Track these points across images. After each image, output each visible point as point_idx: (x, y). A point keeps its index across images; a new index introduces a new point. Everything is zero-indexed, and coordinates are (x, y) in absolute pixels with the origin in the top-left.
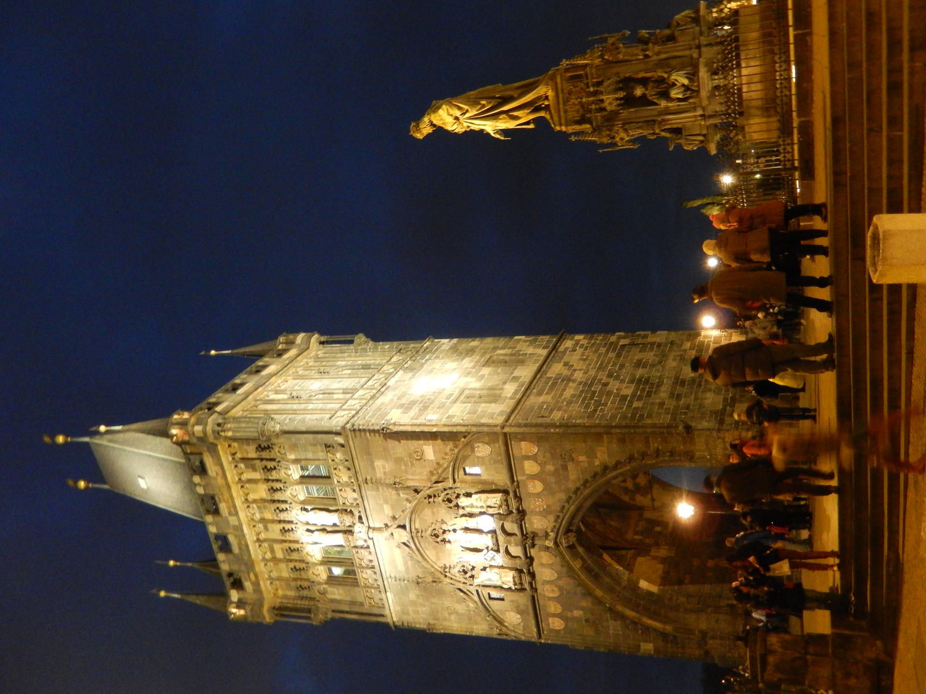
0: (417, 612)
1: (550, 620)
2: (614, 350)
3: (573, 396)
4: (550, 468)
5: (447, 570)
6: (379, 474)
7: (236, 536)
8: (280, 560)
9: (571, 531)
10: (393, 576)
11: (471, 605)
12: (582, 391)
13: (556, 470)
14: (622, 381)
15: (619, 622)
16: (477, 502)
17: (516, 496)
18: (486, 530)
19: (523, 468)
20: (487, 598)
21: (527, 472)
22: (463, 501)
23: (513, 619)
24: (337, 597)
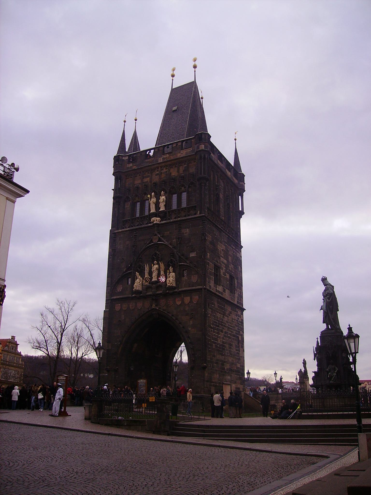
2: (236, 333)
3: (217, 317)
4: (187, 309)
6: (183, 231)
12: (219, 321)
14: (223, 338)
22: (171, 269)
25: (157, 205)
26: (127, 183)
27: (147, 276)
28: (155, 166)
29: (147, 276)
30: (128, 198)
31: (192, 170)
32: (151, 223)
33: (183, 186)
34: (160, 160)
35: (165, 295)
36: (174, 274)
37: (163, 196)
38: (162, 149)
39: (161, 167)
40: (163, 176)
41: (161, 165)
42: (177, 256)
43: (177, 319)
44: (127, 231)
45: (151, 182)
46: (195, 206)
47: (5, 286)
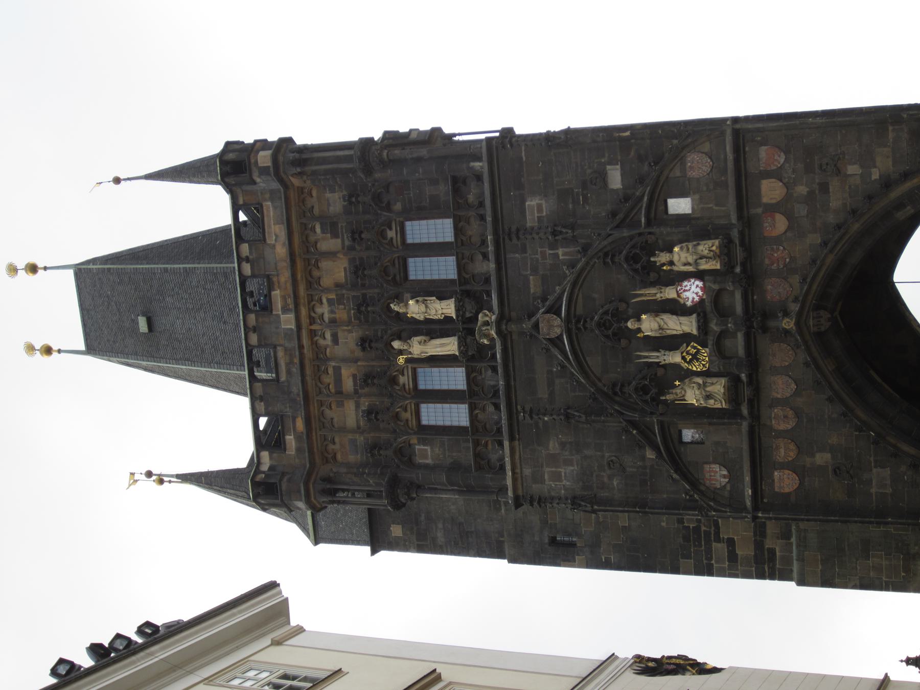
0: (557, 477)
1: (776, 473)
4: (802, 190)
6: (531, 220)
7: (286, 350)
10: (527, 408)
11: (650, 454)
13: (811, 193)
15: (887, 472)
16: (681, 256)
17: (742, 244)
18: (689, 303)
19: (759, 194)
21: (765, 200)
23: (717, 475)
24: (429, 461)
25: (434, 329)
26: (352, 458)
27: (675, 358)
28: (305, 341)
29: (675, 358)
30: (400, 452)
31: (335, 201)
32: (492, 346)
33: (383, 234)
34: (288, 321)
36: (676, 249)
37: (407, 305)
38: (252, 317)
39: (312, 321)
40: (342, 314)
41: (305, 321)
42: (617, 234)
43: (839, 227)
45: (356, 361)
46: (455, 180)
47: (639, 659)
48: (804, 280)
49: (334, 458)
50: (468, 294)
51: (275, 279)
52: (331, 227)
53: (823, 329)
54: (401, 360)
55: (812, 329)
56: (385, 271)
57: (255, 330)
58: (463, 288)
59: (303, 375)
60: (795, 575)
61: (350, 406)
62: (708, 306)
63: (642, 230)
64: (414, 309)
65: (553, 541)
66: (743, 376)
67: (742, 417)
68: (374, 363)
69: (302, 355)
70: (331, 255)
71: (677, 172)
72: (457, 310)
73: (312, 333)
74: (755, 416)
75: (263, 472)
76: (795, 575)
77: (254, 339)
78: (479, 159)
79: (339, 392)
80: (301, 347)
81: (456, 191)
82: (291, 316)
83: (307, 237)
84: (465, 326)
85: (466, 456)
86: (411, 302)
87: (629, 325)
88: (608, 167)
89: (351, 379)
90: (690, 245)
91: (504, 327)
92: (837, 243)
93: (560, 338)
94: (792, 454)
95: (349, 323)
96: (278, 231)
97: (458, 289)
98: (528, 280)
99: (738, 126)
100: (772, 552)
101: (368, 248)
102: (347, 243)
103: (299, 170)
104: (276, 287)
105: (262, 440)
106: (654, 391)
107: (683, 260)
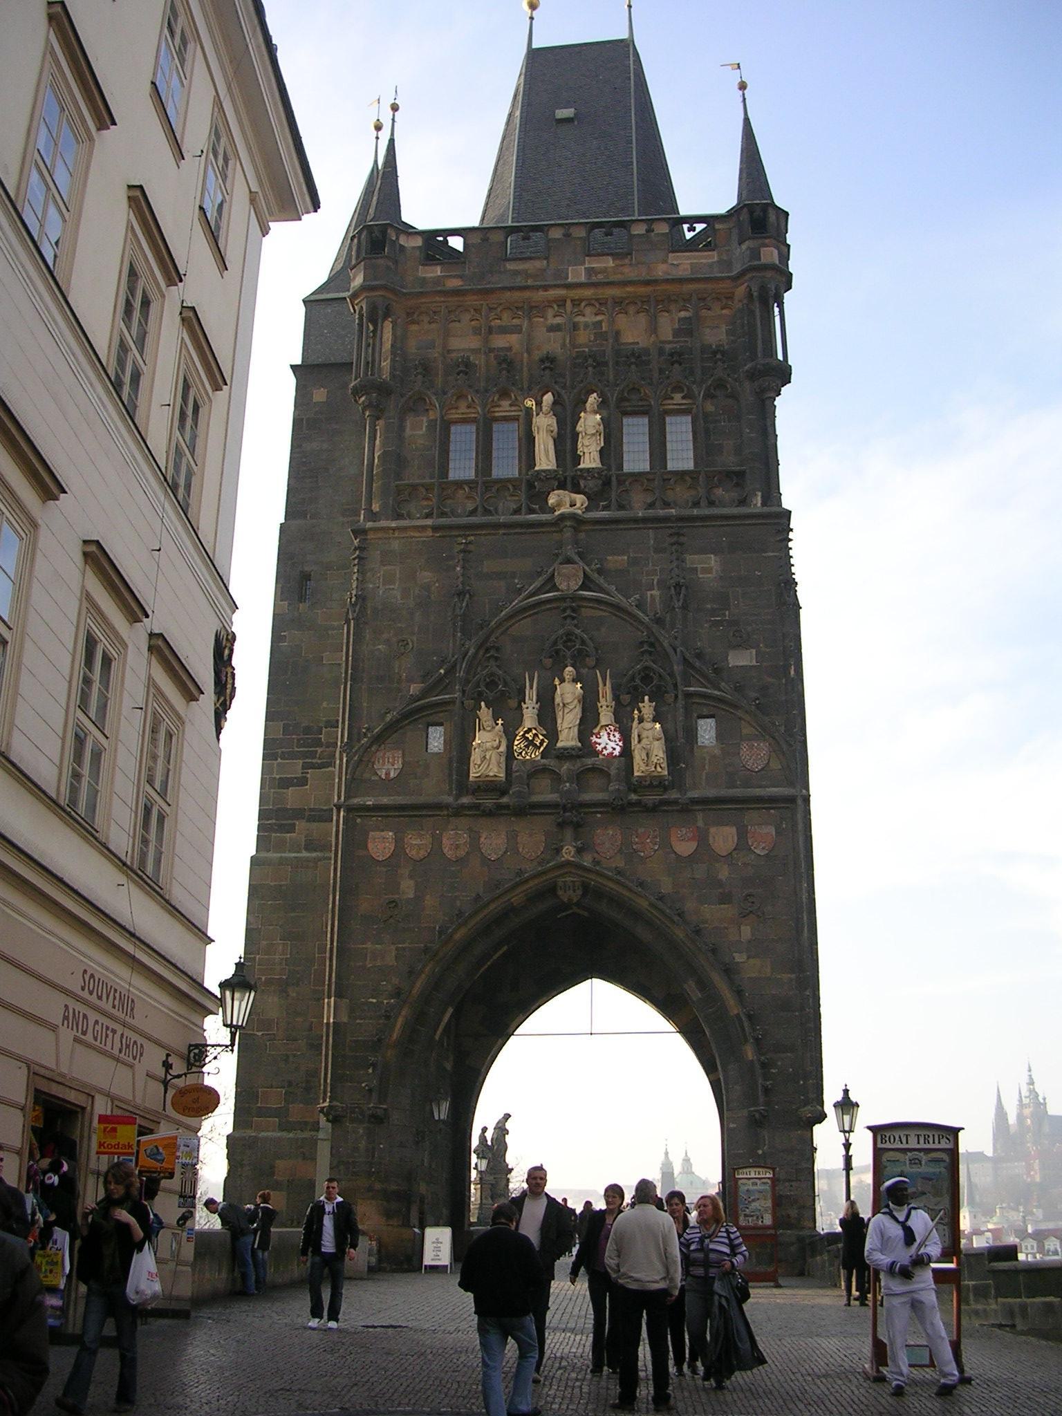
0: (389, 580)
4: (724, 873)
5: (492, 652)
6: (692, 560)
8: (486, 341)
9: (584, 895)
11: (415, 689)
15: (390, 960)
18: (594, 739)
19: (721, 823)
20: (431, 719)
21: (713, 830)
22: (647, 707)
23: (389, 765)
24: (408, 432)
30: (421, 399)
31: (716, 335)
33: (677, 388)
34: (577, 274)
35: (619, 809)
37: (596, 413)
38: (582, 233)
39: (576, 303)
40: (583, 337)
42: (675, 658)
43: (680, 915)
44: (424, 528)
45: (529, 351)
46: (740, 475)
47: (232, 638)
48: (619, 873)
49: (413, 322)
50: (607, 483)
51: (627, 261)
52: (687, 329)
53: (560, 893)
54: (530, 403)
55: (560, 881)
56: (634, 390)
57: (567, 235)
58: (614, 479)
59: (511, 289)
60: (264, 854)
61: (474, 343)
62: (589, 761)
63: (680, 687)
64: (590, 422)
65: (306, 577)
66: (505, 800)
67: (458, 796)
68: (525, 369)
69: (537, 288)
70: (653, 328)
71: (747, 730)
72: (588, 470)
73: (561, 302)
74: (459, 811)
75: (397, 238)
76: (264, 854)
77: (556, 234)
78: (764, 504)
79: (490, 330)
80: (546, 288)
81: (729, 475)
82: (583, 279)
83: (675, 301)
84: (569, 479)
85: (413, 475)
86: (598, 417)
87: (570, 669)
88: (754, 651)
89: (507, 345)
90: (663, 741)
91: (568, 523)
92: (663, 912)
93: (555, 588)
94: (414, 852)
95: (574, 346)
96: (681, 267)
97: (613, 471)
98: (623, 554)
99: (800, 802)
100: (291, 829)
101: (661, 371)
102: (668, 347)
103: (755, 294)
104: (618, 262)
105: (434, 241)
106: (491, 695)
107: (644, 734)
